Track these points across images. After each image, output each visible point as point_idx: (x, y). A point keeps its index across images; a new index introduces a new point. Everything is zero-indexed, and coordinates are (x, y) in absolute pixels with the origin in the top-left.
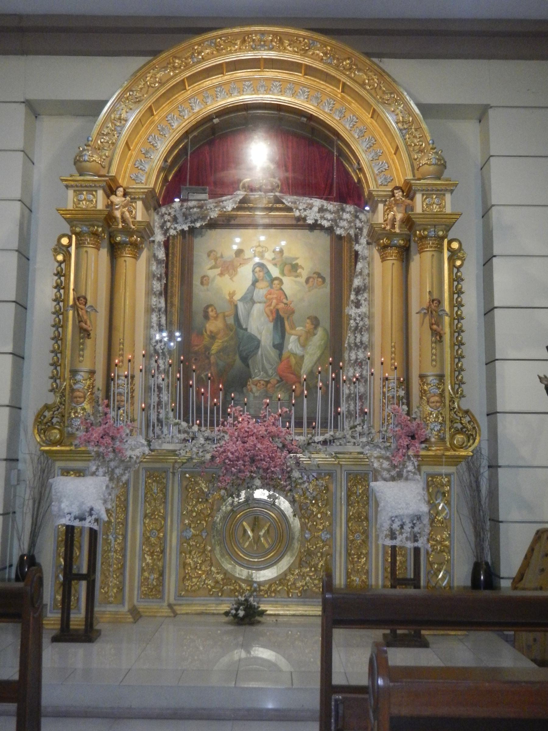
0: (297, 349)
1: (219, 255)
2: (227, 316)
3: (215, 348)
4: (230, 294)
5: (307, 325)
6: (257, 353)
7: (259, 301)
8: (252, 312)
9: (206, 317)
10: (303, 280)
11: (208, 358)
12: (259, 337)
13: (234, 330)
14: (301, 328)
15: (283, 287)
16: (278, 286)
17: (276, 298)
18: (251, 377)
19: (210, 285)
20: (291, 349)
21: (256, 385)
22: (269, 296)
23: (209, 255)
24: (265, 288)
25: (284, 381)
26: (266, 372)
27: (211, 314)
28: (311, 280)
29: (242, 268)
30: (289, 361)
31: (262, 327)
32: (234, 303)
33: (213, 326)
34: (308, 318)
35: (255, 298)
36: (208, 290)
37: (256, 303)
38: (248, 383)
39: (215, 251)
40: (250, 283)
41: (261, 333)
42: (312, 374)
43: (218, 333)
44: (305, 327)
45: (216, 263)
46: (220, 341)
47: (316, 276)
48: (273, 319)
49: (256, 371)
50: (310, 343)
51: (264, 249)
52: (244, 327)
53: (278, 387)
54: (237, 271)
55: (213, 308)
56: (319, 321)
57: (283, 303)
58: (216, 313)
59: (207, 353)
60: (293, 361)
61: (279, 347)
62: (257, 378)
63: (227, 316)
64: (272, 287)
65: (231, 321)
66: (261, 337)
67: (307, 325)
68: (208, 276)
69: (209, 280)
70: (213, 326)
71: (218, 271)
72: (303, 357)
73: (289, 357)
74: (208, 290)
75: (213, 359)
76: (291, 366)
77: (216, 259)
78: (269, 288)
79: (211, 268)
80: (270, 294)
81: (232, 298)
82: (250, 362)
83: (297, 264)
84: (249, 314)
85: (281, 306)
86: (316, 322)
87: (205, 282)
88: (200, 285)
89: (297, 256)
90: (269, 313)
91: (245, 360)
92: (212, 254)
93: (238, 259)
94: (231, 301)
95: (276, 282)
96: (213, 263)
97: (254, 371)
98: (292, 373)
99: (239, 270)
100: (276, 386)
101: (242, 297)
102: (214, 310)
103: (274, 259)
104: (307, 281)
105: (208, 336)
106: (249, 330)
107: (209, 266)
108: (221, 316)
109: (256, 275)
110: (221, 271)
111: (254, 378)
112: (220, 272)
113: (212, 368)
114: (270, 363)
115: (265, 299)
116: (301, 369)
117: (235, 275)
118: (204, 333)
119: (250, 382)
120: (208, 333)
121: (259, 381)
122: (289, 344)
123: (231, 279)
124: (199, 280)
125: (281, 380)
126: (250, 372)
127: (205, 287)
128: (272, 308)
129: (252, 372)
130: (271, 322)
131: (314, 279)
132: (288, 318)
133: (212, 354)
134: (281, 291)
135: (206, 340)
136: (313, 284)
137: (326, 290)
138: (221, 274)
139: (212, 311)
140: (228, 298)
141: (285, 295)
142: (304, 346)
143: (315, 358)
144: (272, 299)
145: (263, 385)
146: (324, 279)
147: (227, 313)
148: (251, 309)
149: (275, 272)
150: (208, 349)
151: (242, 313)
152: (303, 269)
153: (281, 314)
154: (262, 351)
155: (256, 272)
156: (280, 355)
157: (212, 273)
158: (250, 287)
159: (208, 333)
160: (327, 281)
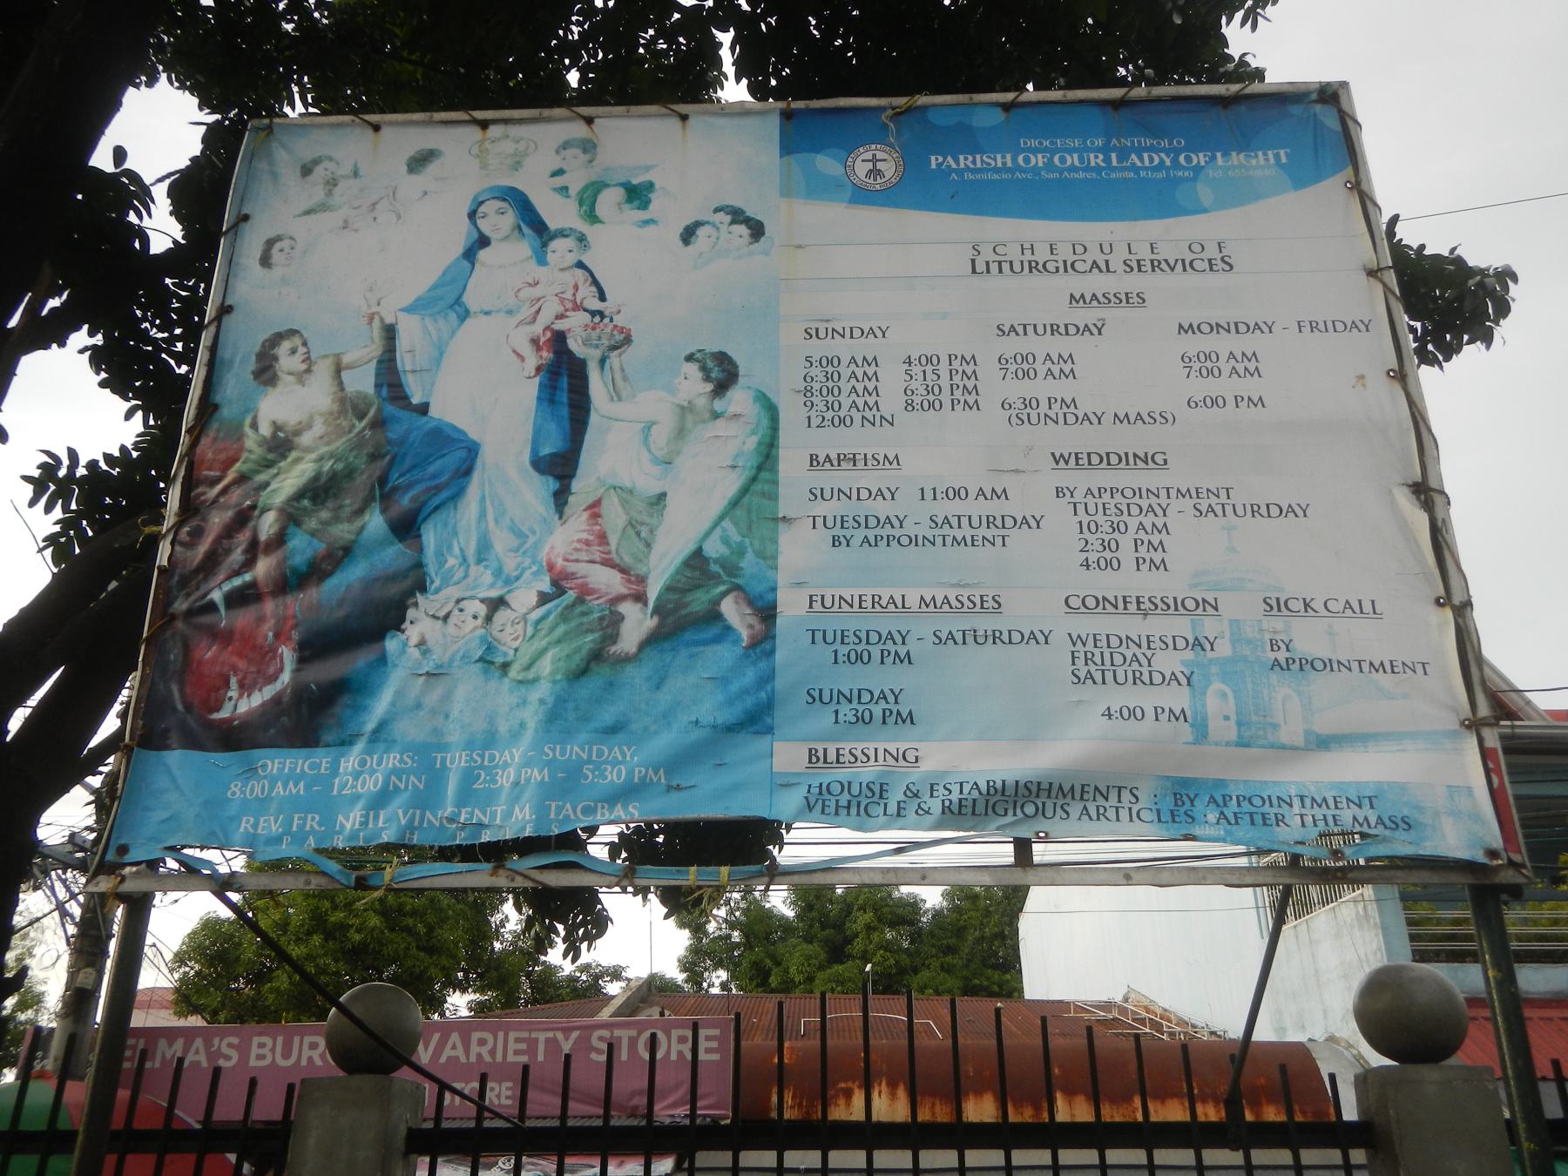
2: (350, 367)
9: (266, 372)
27: (287, 361)
30: (595, 516)
49: (451, 561)
52: (415, 401)
55: (297, 341)
57: (585, 310)
60: (615, 518)
63: (350, 367)
65: (362, 382)
98: (608, 563)
102: (302, 350)
106: (434, 412)
108: (323, 370)
111: (437, 591)
128: (538, 329)
129: (431, 569)
134: (579, 272)
139: (293, 351)
143: (718, 503)
153: (574, 345)
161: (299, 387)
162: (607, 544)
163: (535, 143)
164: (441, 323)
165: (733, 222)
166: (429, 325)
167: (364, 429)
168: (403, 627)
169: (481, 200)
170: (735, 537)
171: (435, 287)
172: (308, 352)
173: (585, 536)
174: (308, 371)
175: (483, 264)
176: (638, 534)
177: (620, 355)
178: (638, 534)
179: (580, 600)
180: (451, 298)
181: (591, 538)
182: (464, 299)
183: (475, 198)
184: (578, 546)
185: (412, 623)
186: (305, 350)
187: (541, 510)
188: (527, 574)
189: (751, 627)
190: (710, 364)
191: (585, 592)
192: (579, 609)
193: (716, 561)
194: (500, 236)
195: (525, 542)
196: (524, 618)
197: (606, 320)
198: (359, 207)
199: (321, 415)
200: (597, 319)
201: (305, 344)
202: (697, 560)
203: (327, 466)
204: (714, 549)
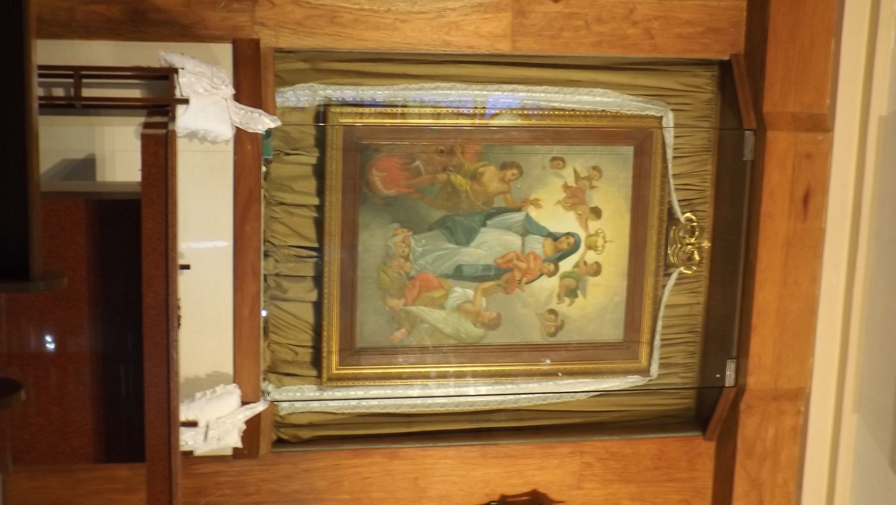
1: (595, 183)
3: (458, 180)
5: (488, 313)
6: (450, 241)
7: (526, 243)
8: (511, 233)
9: (504, 167)
10: (554, 305)
11: (444, 170)
12: (473, 244)
15: (544, 277)
16: (546, 270)
17: (528, 268)
18: (414, 234)
19: (552, 170)
20: (455, 292)
21: (403, 242)
22: (532, 257)
23: (595, 168)
24: (544, 251)
26: (423, 255)
27: (510, 173)
28: (553, 317)
30: (437, 288)
32: (523, 206)
33: (490, 175)
34: (499, 315)
36: (544, 168)
38: (405, 230)
39: (600, 176)
41: (478, 247)
42: (414, 322)
43: (480, 183)
44: (486, 310)
45: (584, 178)
46: (468, 188)
48: (498, 264)
49: (424, 241)
51: (600, 249)
52: (488, 222)
53: (400, 274)
57: (522, 278)
58: (510, 181)
59: (451, 168)
60: (437, 294)
61: (459, 274)
62: (413, 242)
64: (544, 261)
65: (499, 203)
68: (564, 167)
69: (559, 168)
70: (490, 175)
71: (571, 182)
72: (442, 307)
73: (442, 287)
74: (544, 168)
75: (442, 177)
77: (589, 178)
78: (543, 257)
79: (575, 172)
81: (531, 204)
82: (436, 232)
83: (576, 296)
84: (509, 228)
85: (518, 275)
86: (493, 325)
87: (556, 163)
88: (552, 156)
89: (588, 296)
92: (596, 173)
93: (588, 210)
94: (526, 202)
95: (552, 267)
96: (584, 174)
100: (402, 272)
102: (514, 178)
103: (585, 263)
104: (552, 312)
105: (476, 169)
106: (483, 229)
107: (579, 169)
109: (563, 239)
111: (414, 238)
112: (569, 184)
115: (527, 251)
116: (425, 306)
119: (406, 233)
120: (481, 170)
122: (462, 287)
123: (559, 202)
125: (411, 278)
127: (548, 164)
128: (516, 262)
130: (495, 261)
132: (499, 285)
134: (539, 274)
136: (547, 321)
137: (537, 337)
138: (566, 187)
139: (513, 175)
140: (532, 197)
142: (459, 309)
143: (440, 326)
144: (528, 261)
145: (403, 252)
146: (553, 335)
148: (515, 232)
149: (566, 265)
150: (459, 169)
152: (570, 305)
153: (506, 276)
156: (447, 276)
159: (481, 170)
163: (601, 253)
175: (545, 240)
197: (517, 285)
200: (518, 282)
201: (516, 179)
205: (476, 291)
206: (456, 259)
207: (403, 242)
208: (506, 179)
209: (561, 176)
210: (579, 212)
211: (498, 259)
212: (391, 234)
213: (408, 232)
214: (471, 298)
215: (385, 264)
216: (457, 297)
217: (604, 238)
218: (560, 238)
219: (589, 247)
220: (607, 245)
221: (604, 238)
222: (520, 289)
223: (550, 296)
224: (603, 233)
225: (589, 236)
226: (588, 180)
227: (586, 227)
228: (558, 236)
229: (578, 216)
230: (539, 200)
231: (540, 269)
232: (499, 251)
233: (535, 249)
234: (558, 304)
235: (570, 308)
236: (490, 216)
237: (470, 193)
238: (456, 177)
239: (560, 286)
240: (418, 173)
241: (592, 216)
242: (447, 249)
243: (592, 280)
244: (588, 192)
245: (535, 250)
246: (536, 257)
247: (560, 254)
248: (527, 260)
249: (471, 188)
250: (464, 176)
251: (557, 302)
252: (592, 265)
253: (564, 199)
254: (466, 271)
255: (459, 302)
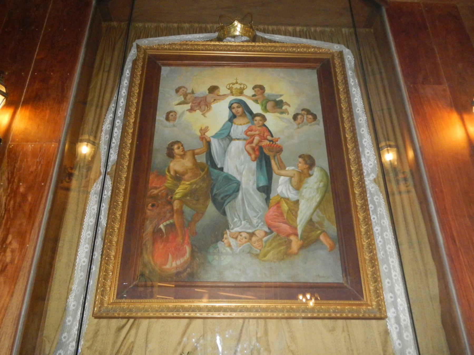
0: (288, 192)
1: (189, 91)
2: (197, 154)
3: (180, 191)
4: (201, 130)
6: (236, 197)
7: (238, 137)
9: (171, 155)
10: (290, 116)
11: (170, 203)
12: (238, 178)
13: (206, 169)
14: (293, 168)
15: (266, 123)
16: (261, 122)
17: (258, 134)
18: (228, 229)
19: (177, 120)
20: (282, 192)
21: (236, 238)
23: (177, 91)
24: (244, 124)
25: (275, 233)
27: (177, 151)
28: (299, 117)
29: (216, 104)
31: (243, 167)
32: (206, 140)
35: (233, 134)
37: (234, 139)
38: (225, 236)
40: (227, 119)
41: (241, 174)
45: (185, 98)
46: (187, 183)
47: (306, 113)
49: (236, 219)
50: (306, 185)
51: (242, 86)
53: (266, 242)
54: (210, 106)
55: (180, 145)
56: (314, 160)
57: (268, 140)
58: (183, 150)
60: (285, 207)
62: (237, 229)
63: (198, 154)
65: (202, 159)
66: (241, 179)
67: (300, 165)
68: (175, 112)
69: (176, 115)
71: (188, 106)
72: (297, 202)
73: (278, 203)
75: (176, 205)
76: (282, 214)
77: (185, 95)
79: (180, 104)
80: (251, 131)
82: (227, 209)
83: (281, 101)
84: (225, 151)
85: (265, 143)
87: (171, 117)
88: (165, 121)
89: (281, 94)
90: (251, 152)
91: (220, 206)
92: (181, 90)
93: (211, 95)
94: (202, 138)
95: (258, 118)
97: (233, 219)
99: (213, 106)
100: (265, 239)
101: (216, 134)
102: (181, 147)
103: (254, 96)
104: (295, 117)
106: (225, 170)
107: (177, 102)
109: (234, 111)
110: (191, 106)
111: (233, 229)
112: (189, 108)
113: (175, 216)
114: (254, 209)
116: (296, 216)
117: (208, 111)
118: (167, 173)
120: (172, 173)
121: (240, 232)
123: (203, 114)
124: (165, 116)
126: (227, 221)
127: (171, 123)
128: (254, 145)
130: (253, 161)
131: (303, 116)
133: (175, 199)
134: (264, 127)
135: (169, 183)
136: (303, 121)
138: (192, 110)
139: (179, 148)
140: (199, 134)
141: (269, 131)
142: (298, 188)
143: (314, 204)
146: (315, 117)
147: (196, 151)
148: (228, 145)
149: (256, 108)
150: (171, 191)
151: (217, 152)
152: (289, 105)
153: (266, 151)
154: (242, 194)
155: (234, 108)
157: (179, 109)
158: (226, 123)
159: (172, 173)
160: (318, 118)
161: (181, 160)
162: (284, 217)
163: (246, 85)
164: (224, 141)
165: (307, 114)
166: (221, 143)
167: (204, 174)
168: (223, 240)
169: (232, 103)
170: (321, 215)
171: (220, 131)
172: (184, 149)
173: (276, 213)
174: (184, 154)
175: (235, 124)
176: (292, 213)
177: (280, 155)
178: (292, 213)
179: (278, 235)
180: (226, 134)
181: (278, 214)
182: (230, 134)
183: (230, 102)
184: (275, 217)
185: (226, 239)
186: (183, 148)
187: (262, 204)
188: (260, 225)
189: (330, 244)
190: (307, 159)
191: (279, 232)
192: (278, 238)
193: (317, 223)
194: (239, 115)
195: (258, 214)
196: (261, 240)
197: (274, 143)
198: (195, 103)
199: (190, 169)
200: (271, 143)
201: (182, 146)
202: (310, 222)
203: (195, 186)
204: (315, 219)
205: (281, 176)
206: (252, 193)
207: (236, 238)
208: (182, 153)
209: (183, 113)
210: (213, 100)
211: (251, 158)
212: (228, 249)
213: (226, 233)
214: (288, 178)
215: (257, 255)
216: (286, 191)
217: (233, 84)
218: (233, 113)
219: (241, 93)
220: (239, 82)
221: (233, 84)
222: (277, 141)
223: (282, 119)
224: (229, 84)
225: (232, 94)
226: (187, 96)
227: (225, 96)
228: (232, 114)
229: (216, 101)
230: (201, 128)
231: (259, 126)
232: (245, 157)
233: (243, 130)
234: (288, 114)
235: (291, 105)
236: (214, 165)
237: (193, 181)
238: (177, 193)
239: (275, 112)
240: (171, 227)
241: (216, 92)
242: (243, 200)
243: (268, 91)
244: (196, 95)
245: (244, 130)
246: (250, 130)
247: (247, 113)
248: (253, 136)
249: (188, 181)
250: (177, 186)
251: (287, 114)
252: (255, 91)
253: (201, 111)
254: (263, 183)
255: (291, 187)
